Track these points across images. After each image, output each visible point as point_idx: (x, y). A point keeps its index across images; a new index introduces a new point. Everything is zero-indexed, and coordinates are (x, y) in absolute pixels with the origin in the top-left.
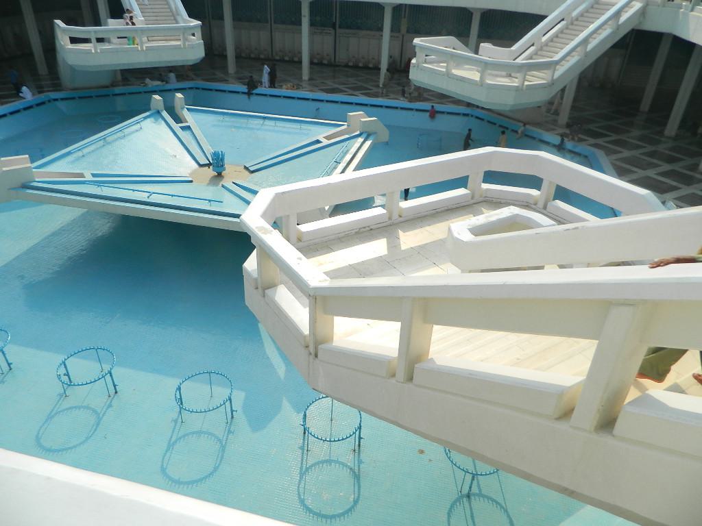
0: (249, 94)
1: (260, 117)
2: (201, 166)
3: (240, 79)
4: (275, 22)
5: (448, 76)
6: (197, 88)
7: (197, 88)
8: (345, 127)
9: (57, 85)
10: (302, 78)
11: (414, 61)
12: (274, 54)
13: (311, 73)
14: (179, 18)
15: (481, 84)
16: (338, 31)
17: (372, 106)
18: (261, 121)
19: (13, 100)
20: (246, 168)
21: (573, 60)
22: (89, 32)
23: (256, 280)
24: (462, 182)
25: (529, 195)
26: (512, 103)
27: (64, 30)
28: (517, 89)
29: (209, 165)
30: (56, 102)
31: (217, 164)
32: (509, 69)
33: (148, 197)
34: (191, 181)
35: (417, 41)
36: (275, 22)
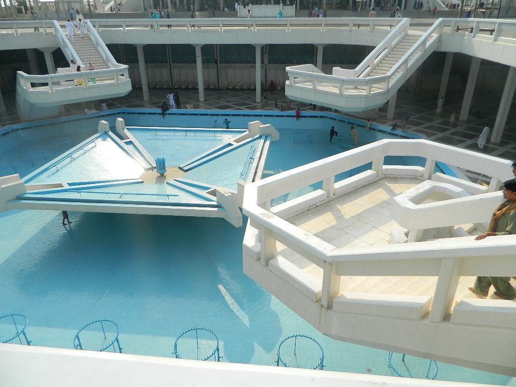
0: (163, 114)
3: (154, 104)
4: (173, 62)
6: (123, 113)
7: (123, 113)
9: (16, 119)
11: (287, 82)
12: (173, 84)
13: (205, 96)
14: (110, 64)
15: (341, 95)
16: (220, 65)
17: (265, 116)
18: (184, 134)
20: (181, 169)
21: (399, 75)
22: (47, 78)
23: (259, 254)
24: (368, 166)
25: (416, 170)
27: (27, 78)
28: (366, 97)
30: (18, 132)
31: (161, 166)
32: (356, 84)
33: (120, 197)
34: (142, 182)
35: (288, 68)
36: (173, 62)
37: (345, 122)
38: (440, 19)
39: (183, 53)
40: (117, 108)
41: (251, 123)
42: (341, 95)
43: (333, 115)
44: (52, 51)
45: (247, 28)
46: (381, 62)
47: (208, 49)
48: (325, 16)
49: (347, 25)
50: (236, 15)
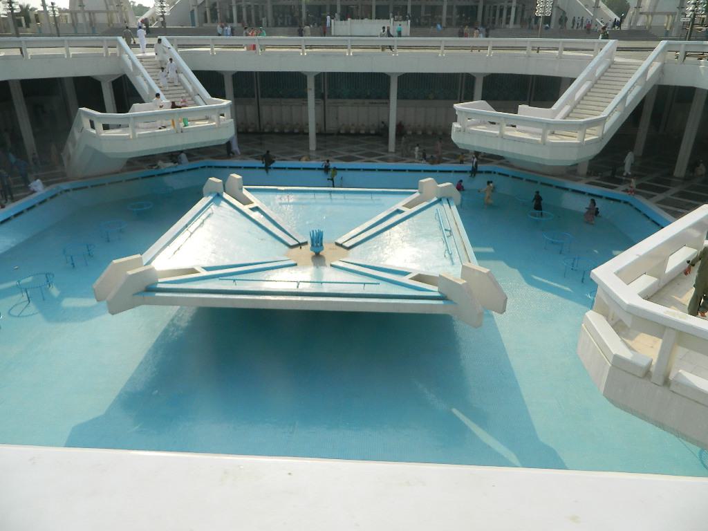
0: (267, 168)
1: (325, 191)
2: (292, 247)
4: (262, 96)
5: (502, 137)
6: (209, 167)
7: (209, 167)
8: (417, 194)
10: (309, 149)
11: (456, 125)
12: (262, 127)
13: (318, 141)
14: (198, 98)
16: (328, 101)
18: (327, 196)
19: (21, 194)
20: (341, 245)
26: (575, 159)
28: (579, 146)
29: (300, 245)
30: (68, 193)
34: (296, 265)
36: (262, 96)
38: (663, 43)
39: (285, 85)
40: (196, 160)
41: (421, 181)
42: (544, 143)
43: (505, 170)
44: (113, 79)
46: (582, 99)
47: (319, 77)
48: (487, 36)
49: (524, 48)
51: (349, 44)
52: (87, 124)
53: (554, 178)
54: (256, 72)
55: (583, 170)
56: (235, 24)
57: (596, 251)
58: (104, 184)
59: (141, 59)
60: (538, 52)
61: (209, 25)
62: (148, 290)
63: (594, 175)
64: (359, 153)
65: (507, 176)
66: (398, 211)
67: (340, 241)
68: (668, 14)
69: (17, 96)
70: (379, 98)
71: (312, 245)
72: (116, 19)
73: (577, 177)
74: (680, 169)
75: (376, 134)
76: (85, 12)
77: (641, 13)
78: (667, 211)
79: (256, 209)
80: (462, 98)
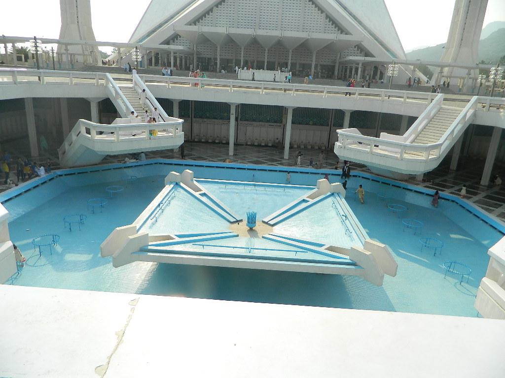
8: (316, 190)
11: (337, 144)
12: (193, 138)
13: (235, 150)
18: (253, 187)
20: (267, 223)
21: (447, 142)
26: (423, 171)
28: (426, 161)
29: (238, 222)
30: (61, 177)
34: (238, 236)
35: (338, 131)
36: (195, 117)
37: (389, 184)
38: (475, 98)
40: (151, 158)
45: (283, 92)
46: (422, 131)
50: (236, 78)
51: (263, 86)
52: (83, 131)
53: (402, 182)
54: (192, 101)
55: (421, 178)
56: (172, 68)
57: (439, 235)
58: (87, 172)
59: (121, 88)
60: (389, 98)
61: (153, 67)
62: (142, 250)
63: (428, 182)
64: (264, 158)
65: (369, 179)
66: (304, 201)
67: (266, 220)
68: (461, 78)
69: (29, 109)
70: (275, 122)
71: (248, 222)
72: (90, 60)
73: (415, 182)
74: (485, 180)
75: (272, 146)
76: (68, 54)
77: (443, 76)
78: (482, 208)
79: (204, 195)
80: (379, 128)
